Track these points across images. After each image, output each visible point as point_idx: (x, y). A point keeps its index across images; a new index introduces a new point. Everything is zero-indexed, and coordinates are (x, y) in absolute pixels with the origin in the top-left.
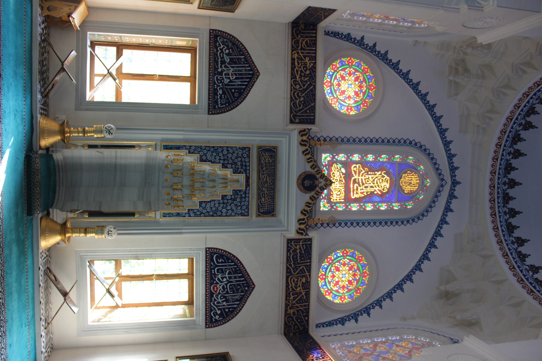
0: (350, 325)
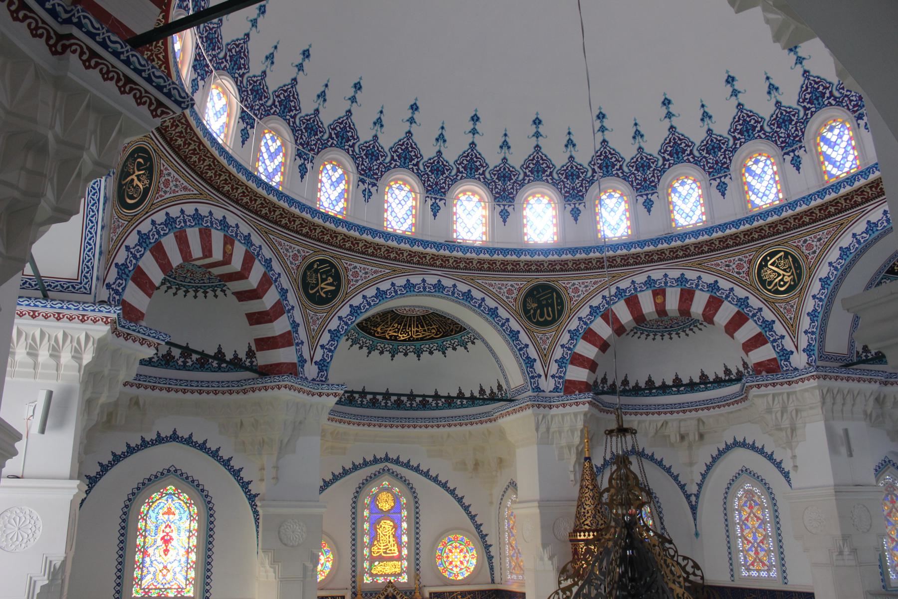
0: (493, 551)
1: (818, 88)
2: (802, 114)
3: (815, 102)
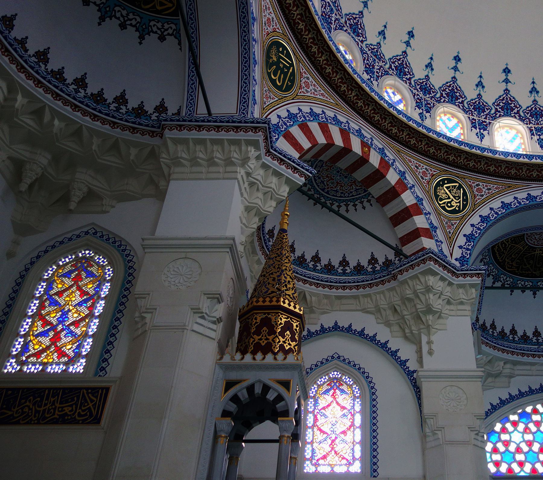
1: (511, 104)
2: (493, 111)
3: (505, 110)
